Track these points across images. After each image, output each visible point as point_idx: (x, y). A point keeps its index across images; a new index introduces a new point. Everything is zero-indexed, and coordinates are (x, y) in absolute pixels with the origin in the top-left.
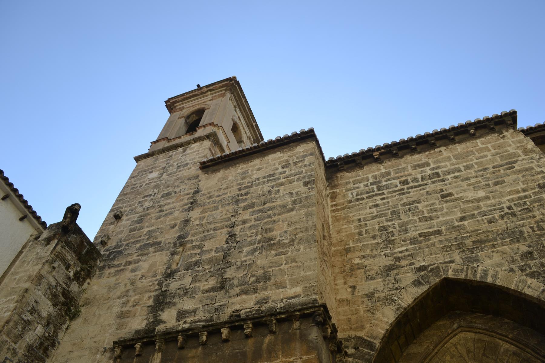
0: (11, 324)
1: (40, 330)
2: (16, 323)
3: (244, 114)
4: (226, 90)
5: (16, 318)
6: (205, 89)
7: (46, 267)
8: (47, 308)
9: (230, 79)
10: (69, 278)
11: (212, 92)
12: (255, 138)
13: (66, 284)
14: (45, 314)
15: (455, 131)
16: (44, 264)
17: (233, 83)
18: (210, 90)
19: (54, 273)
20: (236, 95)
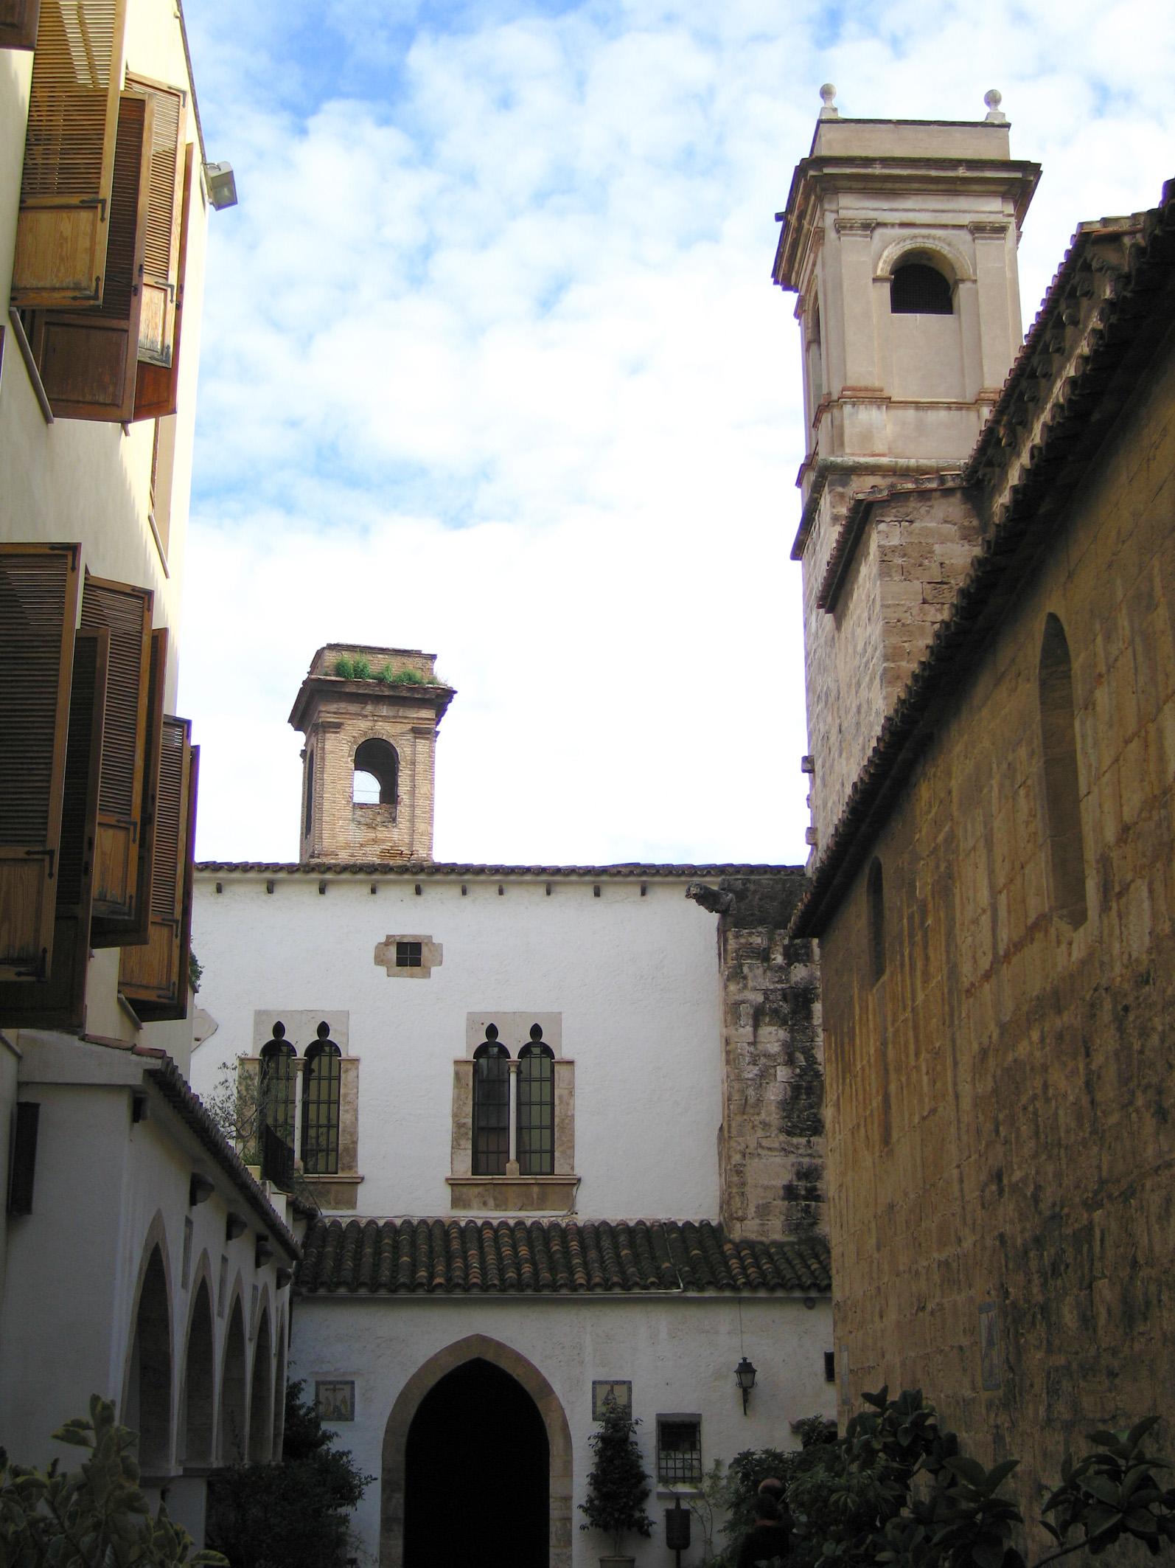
0: (736, 1097)
1: (782, 1073)
2: (742, 1091)
3: (916, 186)
4: (820, 200)
5: (736, 1085)
6: (793, 220)
7: (733, 987)
8: (773, 1038)
9: (801, 171)
10: (781, 967)
11: (808, 217)
12: (1002, 189)
13: (780, 981)
14: (774, 1048)
15: (1051, 324)
16: (726, 987)
17: (813, 177)
18: (801, 217)
19: (750, 984)
20: (846, 183)
